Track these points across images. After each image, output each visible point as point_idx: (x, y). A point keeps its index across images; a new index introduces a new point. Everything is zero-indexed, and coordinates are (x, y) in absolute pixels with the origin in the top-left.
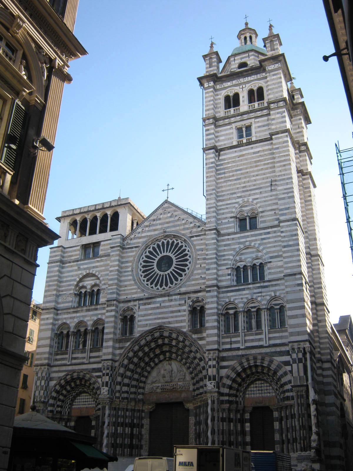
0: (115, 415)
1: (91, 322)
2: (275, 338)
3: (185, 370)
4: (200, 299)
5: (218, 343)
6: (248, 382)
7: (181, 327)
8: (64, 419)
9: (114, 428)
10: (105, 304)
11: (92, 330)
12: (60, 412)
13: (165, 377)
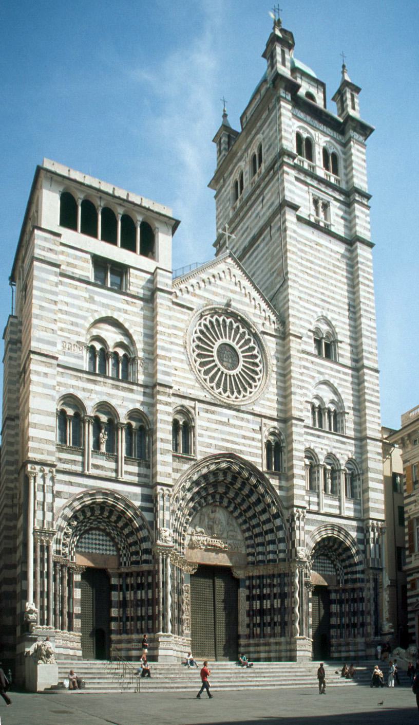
4: (277, 431)
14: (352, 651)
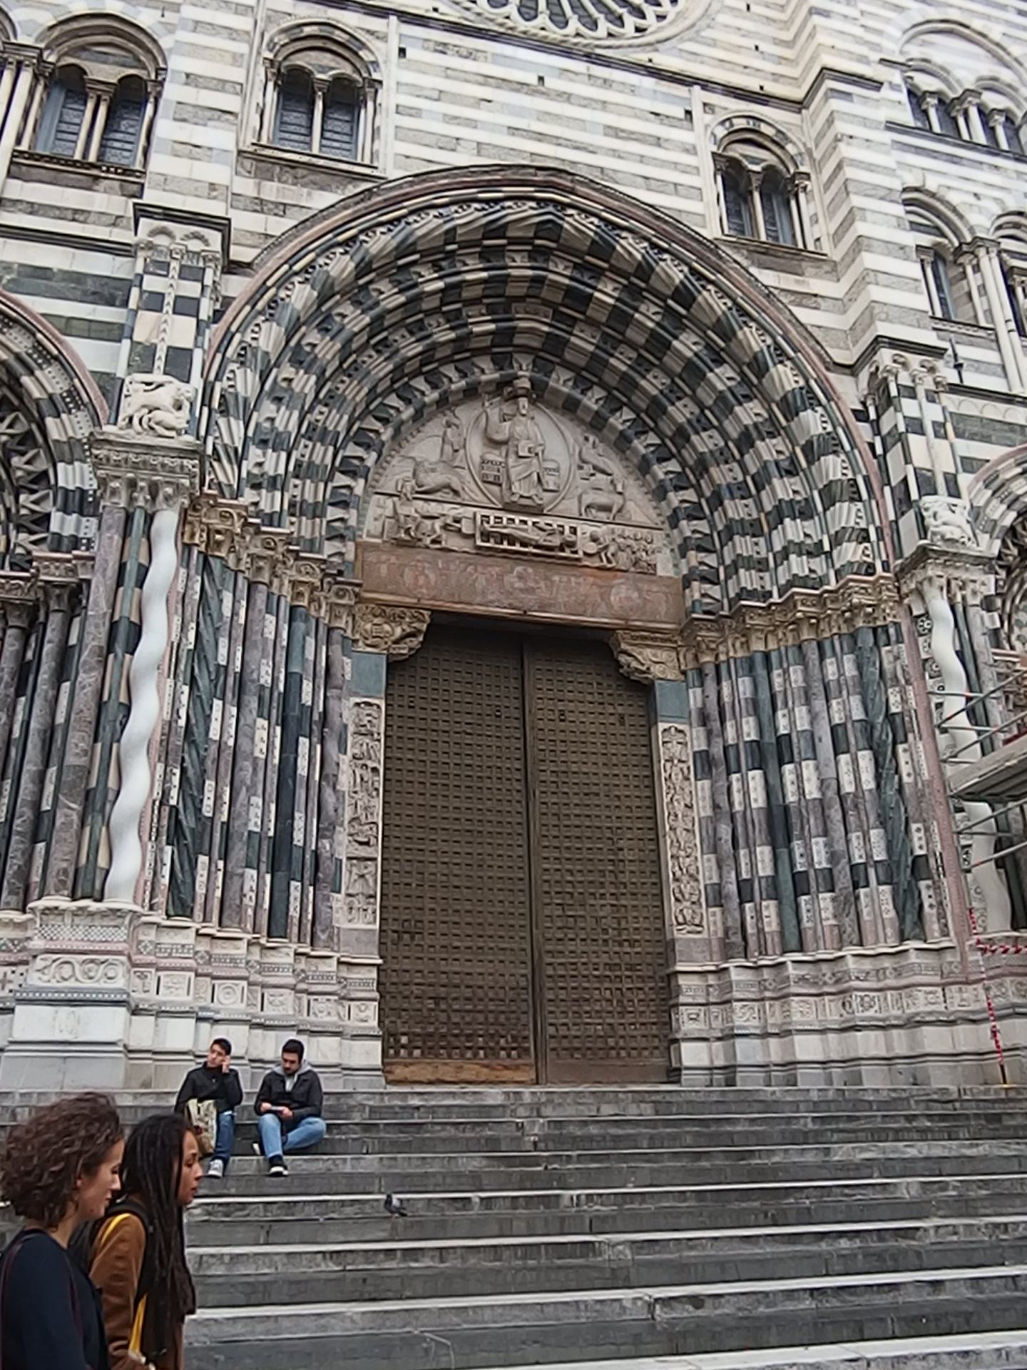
9: (184, 698)
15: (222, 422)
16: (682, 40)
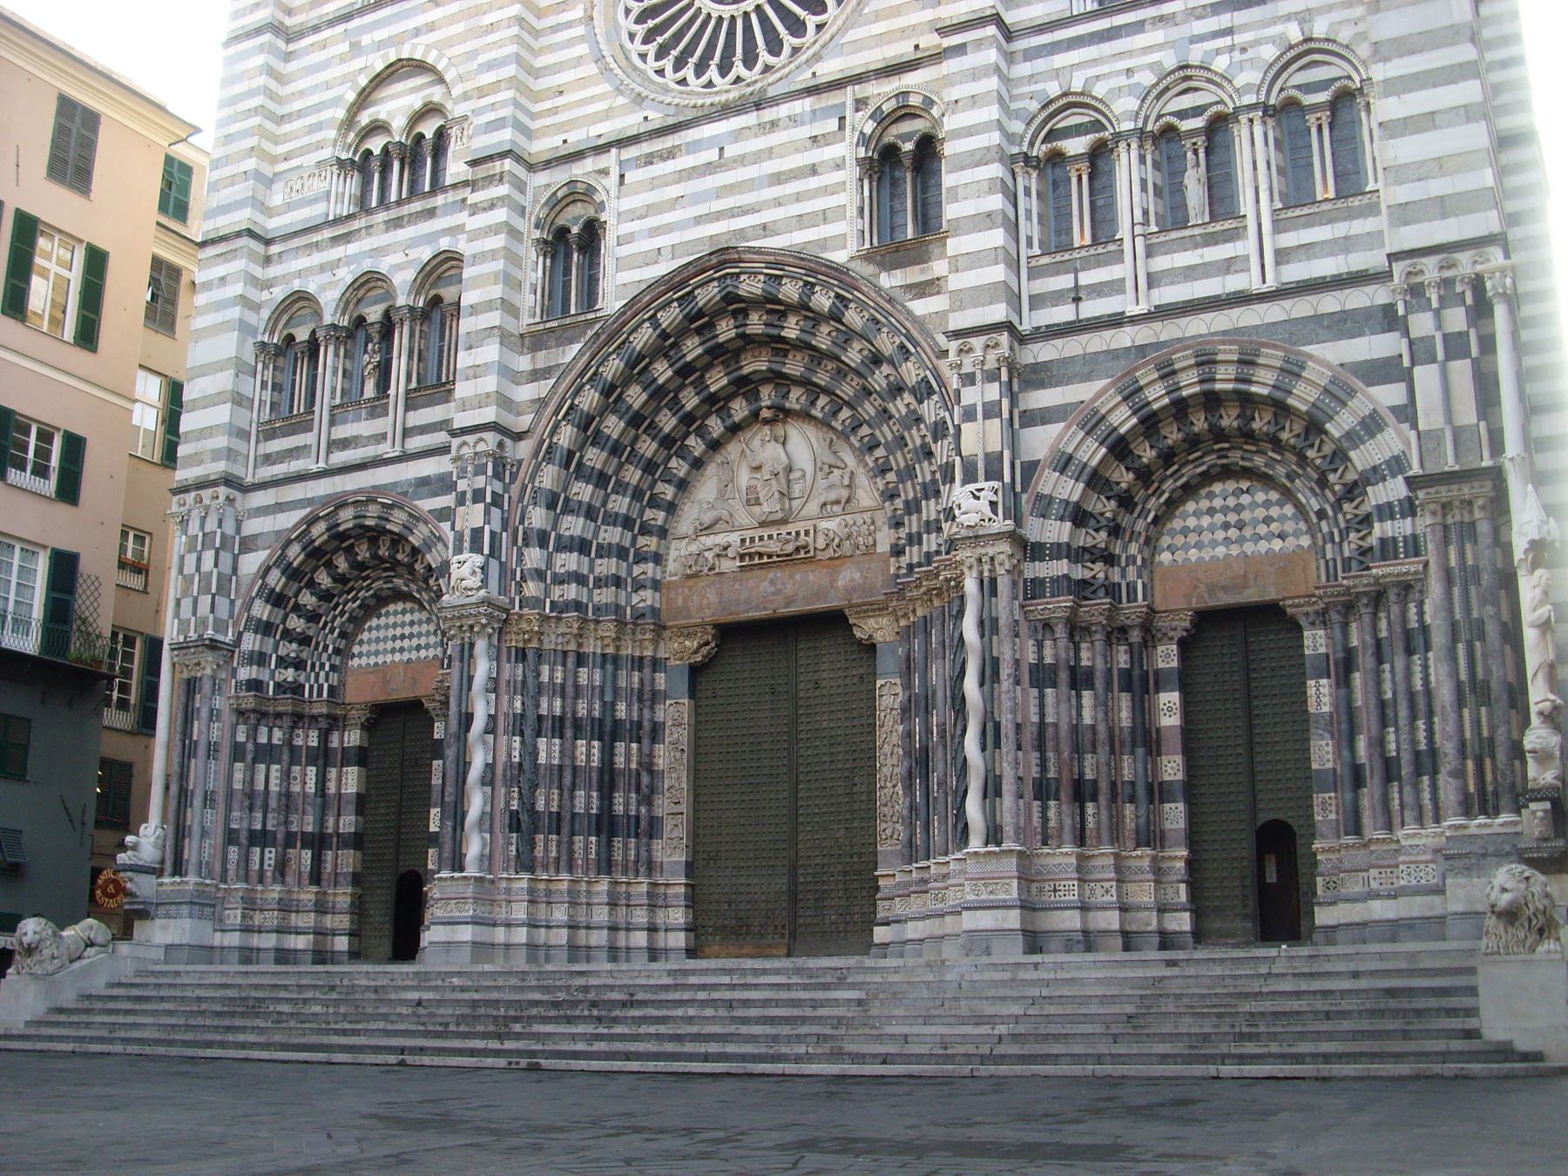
0: (524, 682)
1: (410, 274)
2: (1308, 250)
3: (850, 459)
4: (914, 100)
5: (1014, 299)
6: (1168, 485)
7: (824, 243)
8: (314, 718)
9: (517, 745)
10: (466, 183)
11: (412, 309)
12: (297, 688)
13: (757, 502)
14: (1376, 896)
15: (526, 551)
16: (847, 30)
